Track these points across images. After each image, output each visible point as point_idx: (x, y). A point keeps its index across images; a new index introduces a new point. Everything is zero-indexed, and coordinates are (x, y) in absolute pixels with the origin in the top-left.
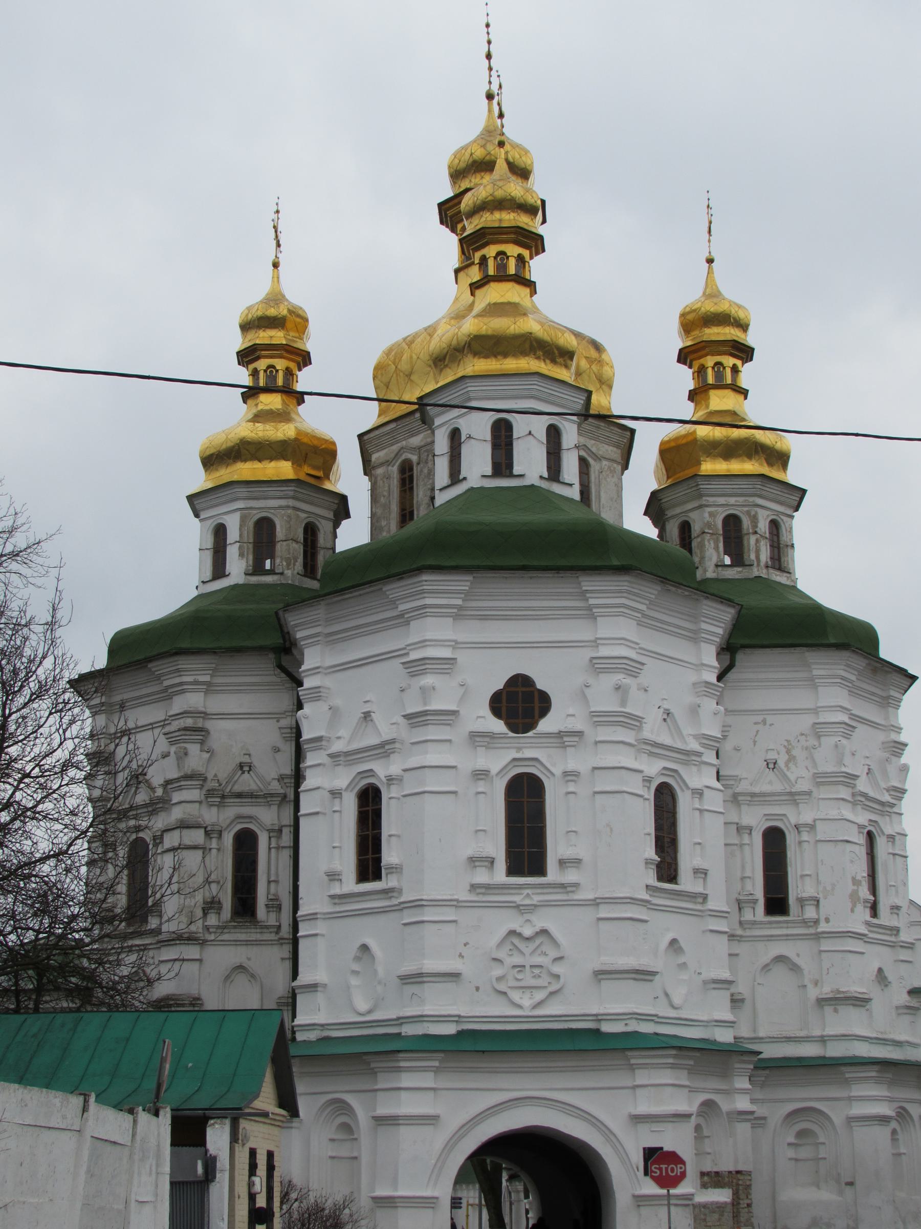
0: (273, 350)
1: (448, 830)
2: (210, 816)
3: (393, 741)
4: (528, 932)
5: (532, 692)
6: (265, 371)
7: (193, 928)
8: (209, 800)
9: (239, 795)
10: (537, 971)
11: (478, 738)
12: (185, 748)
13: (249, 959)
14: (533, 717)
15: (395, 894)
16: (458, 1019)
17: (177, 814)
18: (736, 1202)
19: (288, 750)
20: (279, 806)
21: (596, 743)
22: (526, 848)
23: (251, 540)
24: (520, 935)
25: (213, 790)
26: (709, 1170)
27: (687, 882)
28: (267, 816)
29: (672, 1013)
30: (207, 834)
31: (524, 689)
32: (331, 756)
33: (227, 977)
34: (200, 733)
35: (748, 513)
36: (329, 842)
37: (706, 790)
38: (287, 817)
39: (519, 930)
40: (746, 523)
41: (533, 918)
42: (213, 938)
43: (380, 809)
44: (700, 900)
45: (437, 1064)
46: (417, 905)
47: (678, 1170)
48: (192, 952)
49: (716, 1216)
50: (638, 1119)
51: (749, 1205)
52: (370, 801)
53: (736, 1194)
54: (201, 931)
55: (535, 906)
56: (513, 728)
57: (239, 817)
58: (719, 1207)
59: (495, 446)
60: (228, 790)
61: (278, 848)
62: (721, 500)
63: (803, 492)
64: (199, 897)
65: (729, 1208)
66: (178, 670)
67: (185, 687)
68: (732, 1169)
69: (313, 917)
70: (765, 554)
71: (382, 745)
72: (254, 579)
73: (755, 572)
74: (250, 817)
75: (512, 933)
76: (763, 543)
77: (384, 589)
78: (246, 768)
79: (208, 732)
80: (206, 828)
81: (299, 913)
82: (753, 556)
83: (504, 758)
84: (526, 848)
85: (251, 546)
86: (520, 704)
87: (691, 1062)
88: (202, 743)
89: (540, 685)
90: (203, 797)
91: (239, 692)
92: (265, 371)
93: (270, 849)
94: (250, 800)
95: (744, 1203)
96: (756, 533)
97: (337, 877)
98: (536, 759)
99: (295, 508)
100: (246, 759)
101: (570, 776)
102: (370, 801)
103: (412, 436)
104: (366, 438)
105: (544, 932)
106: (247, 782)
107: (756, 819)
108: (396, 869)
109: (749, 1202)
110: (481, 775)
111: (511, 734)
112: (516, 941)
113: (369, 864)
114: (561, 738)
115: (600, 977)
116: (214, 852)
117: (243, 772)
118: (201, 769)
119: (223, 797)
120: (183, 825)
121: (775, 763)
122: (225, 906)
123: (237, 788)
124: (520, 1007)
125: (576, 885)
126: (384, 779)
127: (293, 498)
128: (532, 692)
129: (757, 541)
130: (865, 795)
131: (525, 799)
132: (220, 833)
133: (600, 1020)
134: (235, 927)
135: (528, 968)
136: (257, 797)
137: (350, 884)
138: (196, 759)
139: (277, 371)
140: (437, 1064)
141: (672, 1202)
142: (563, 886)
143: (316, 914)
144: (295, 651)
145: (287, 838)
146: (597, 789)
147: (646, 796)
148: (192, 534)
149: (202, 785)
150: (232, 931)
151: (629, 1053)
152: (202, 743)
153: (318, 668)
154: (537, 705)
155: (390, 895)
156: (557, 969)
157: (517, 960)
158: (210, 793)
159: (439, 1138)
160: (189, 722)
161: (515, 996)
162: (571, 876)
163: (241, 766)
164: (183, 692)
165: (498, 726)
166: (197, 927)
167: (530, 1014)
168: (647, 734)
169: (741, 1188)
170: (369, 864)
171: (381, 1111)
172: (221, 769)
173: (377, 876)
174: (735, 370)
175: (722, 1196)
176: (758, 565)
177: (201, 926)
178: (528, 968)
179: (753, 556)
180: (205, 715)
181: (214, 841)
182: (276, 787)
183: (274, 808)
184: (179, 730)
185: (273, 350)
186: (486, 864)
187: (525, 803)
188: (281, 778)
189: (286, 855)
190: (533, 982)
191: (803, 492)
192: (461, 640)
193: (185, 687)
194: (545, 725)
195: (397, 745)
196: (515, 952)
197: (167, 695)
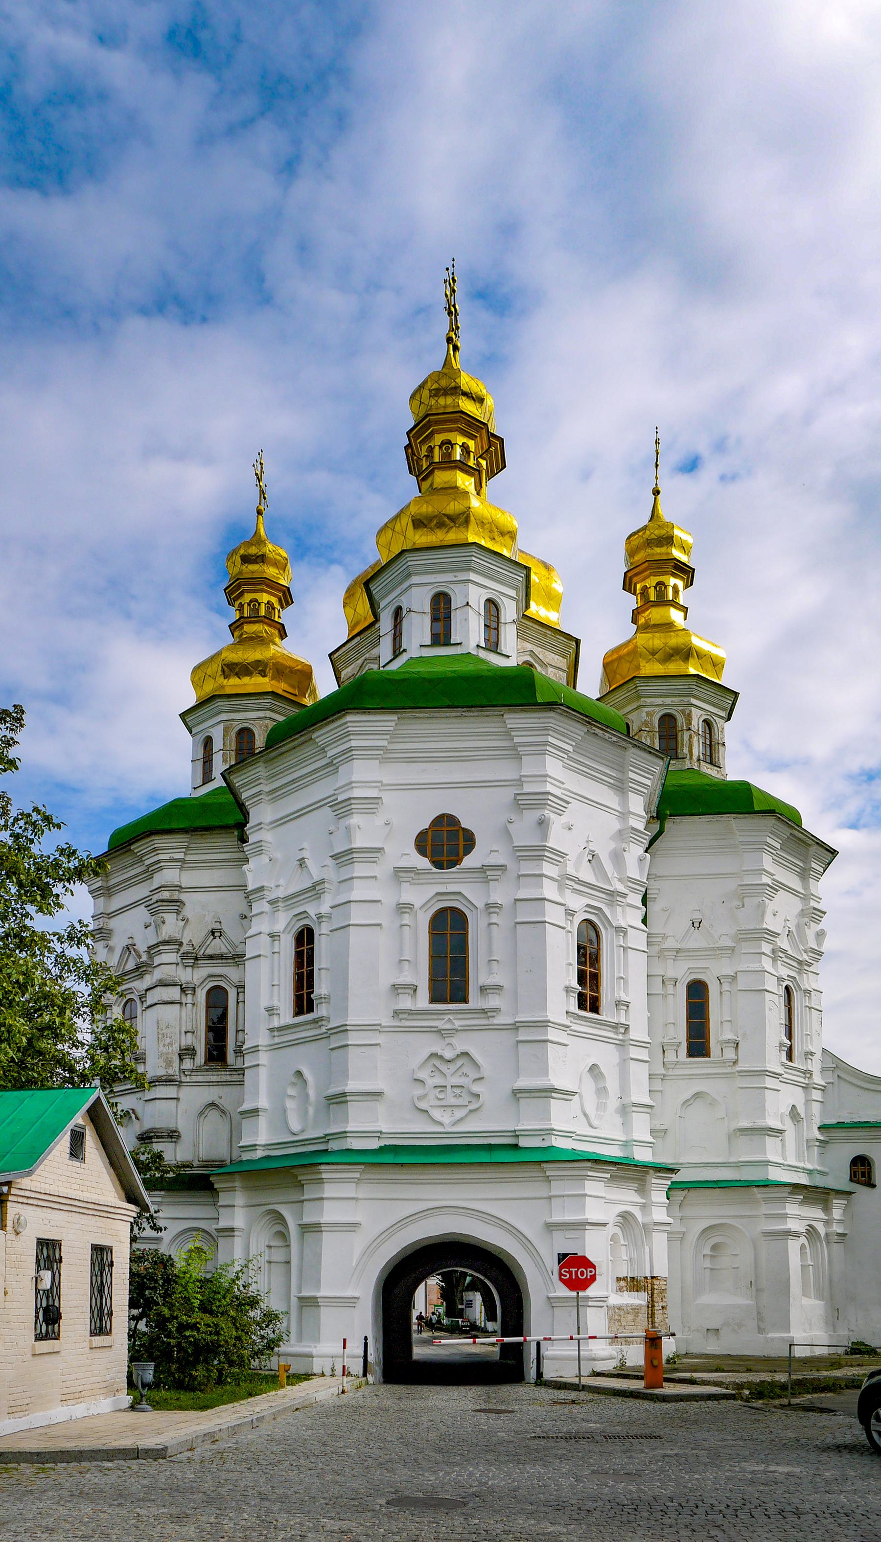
2: (185, 975)
3: (322, 882)
4: (448, 1054)
9: (211, 957)
10: (458, 1091)
11: (400, 874)
14: (458, 855)
15: (324, 1023)
16: (379, 1135)
18: (651, 1305)
21: (519, 876)
22: (450, 976)
25: (187, 953)
27: (607, 1013)
30: (183, 990)
32: (271, 902)
35: (683, 712)
37: (629, 929)
39: (440, 1053)
40: (681, 720)
41: (454, 1041)
44: (622, 1030)
45: (357, 1175)
46: (342, 1030)
47: (588, 1273)
49: (630, 1317)
50: (551, 1227)
55: (457, 1030)
56: (438, 865)
58: (636, 1310)
60: (201, 953)
62: (659, 701)
64: (176, 1048)
65: (644, 1310)
69: (255, 1049)
70: (698, 749)
71: (313, 887)
73: (687, 764)
75: (434, 1055)
76: (695, 739)
79: (182, 902)
80: (181, 985)
82: (686, 751)
83: (426, 893)
84: (450, 976)
87: (608, 1176)
88: (178, 912)
90: (179, 959)
91: (211, 868)
95: (658, 1306)
96: (690, 729)
97: (275, 1012)
98: (460, 893)
100: (217, 926)
101: (490, 907)
105: (466, 1054)
107: (683, 972)
108: (327, 998)
109: (664, 1304)
110: (403, 908)
111: (435, 870)
112: (437, 1063)
114: (484, 872)
115: (518, 1095)
118: (177, 936)
120: (163, 984)
123: (209, 952)
124: (441, 1124)
125: (497, 1010)
126: (315, 918)
129: (690, 736)
130: (784, 951)
133: (517, 1136)
135: (449, 1087)
137: (286, 1016)
138: (171, 926)
140: (357, 1175)
142: (484, 1011)
143: (258, 1046)
146: (518, 920)
147: (569, 928)
148: (184, 744)
151: (544, 1165)
152: (178, 912)
155: (320, 1023)
156: (476, 1088)
157: (438, 1081)
158: (185, 956)
159: (359, 1242)
161: (436, 1114)
162: (493, 1001)
165: (424, 863)
167: (450, 1130)
168: (571, 870)
169: (656, 1291)
171: (307, 1220)
172: (193, 935)
173: (311, 1009)
176: (691, 758)
178: (449, 1087)
179: (686, 751)
186: (409, 991)
187: (449, 934)
190: (453, 1101)
192: (390, 781)
194: (469, 861)
196: (437, 1074)
197: (149, 873)
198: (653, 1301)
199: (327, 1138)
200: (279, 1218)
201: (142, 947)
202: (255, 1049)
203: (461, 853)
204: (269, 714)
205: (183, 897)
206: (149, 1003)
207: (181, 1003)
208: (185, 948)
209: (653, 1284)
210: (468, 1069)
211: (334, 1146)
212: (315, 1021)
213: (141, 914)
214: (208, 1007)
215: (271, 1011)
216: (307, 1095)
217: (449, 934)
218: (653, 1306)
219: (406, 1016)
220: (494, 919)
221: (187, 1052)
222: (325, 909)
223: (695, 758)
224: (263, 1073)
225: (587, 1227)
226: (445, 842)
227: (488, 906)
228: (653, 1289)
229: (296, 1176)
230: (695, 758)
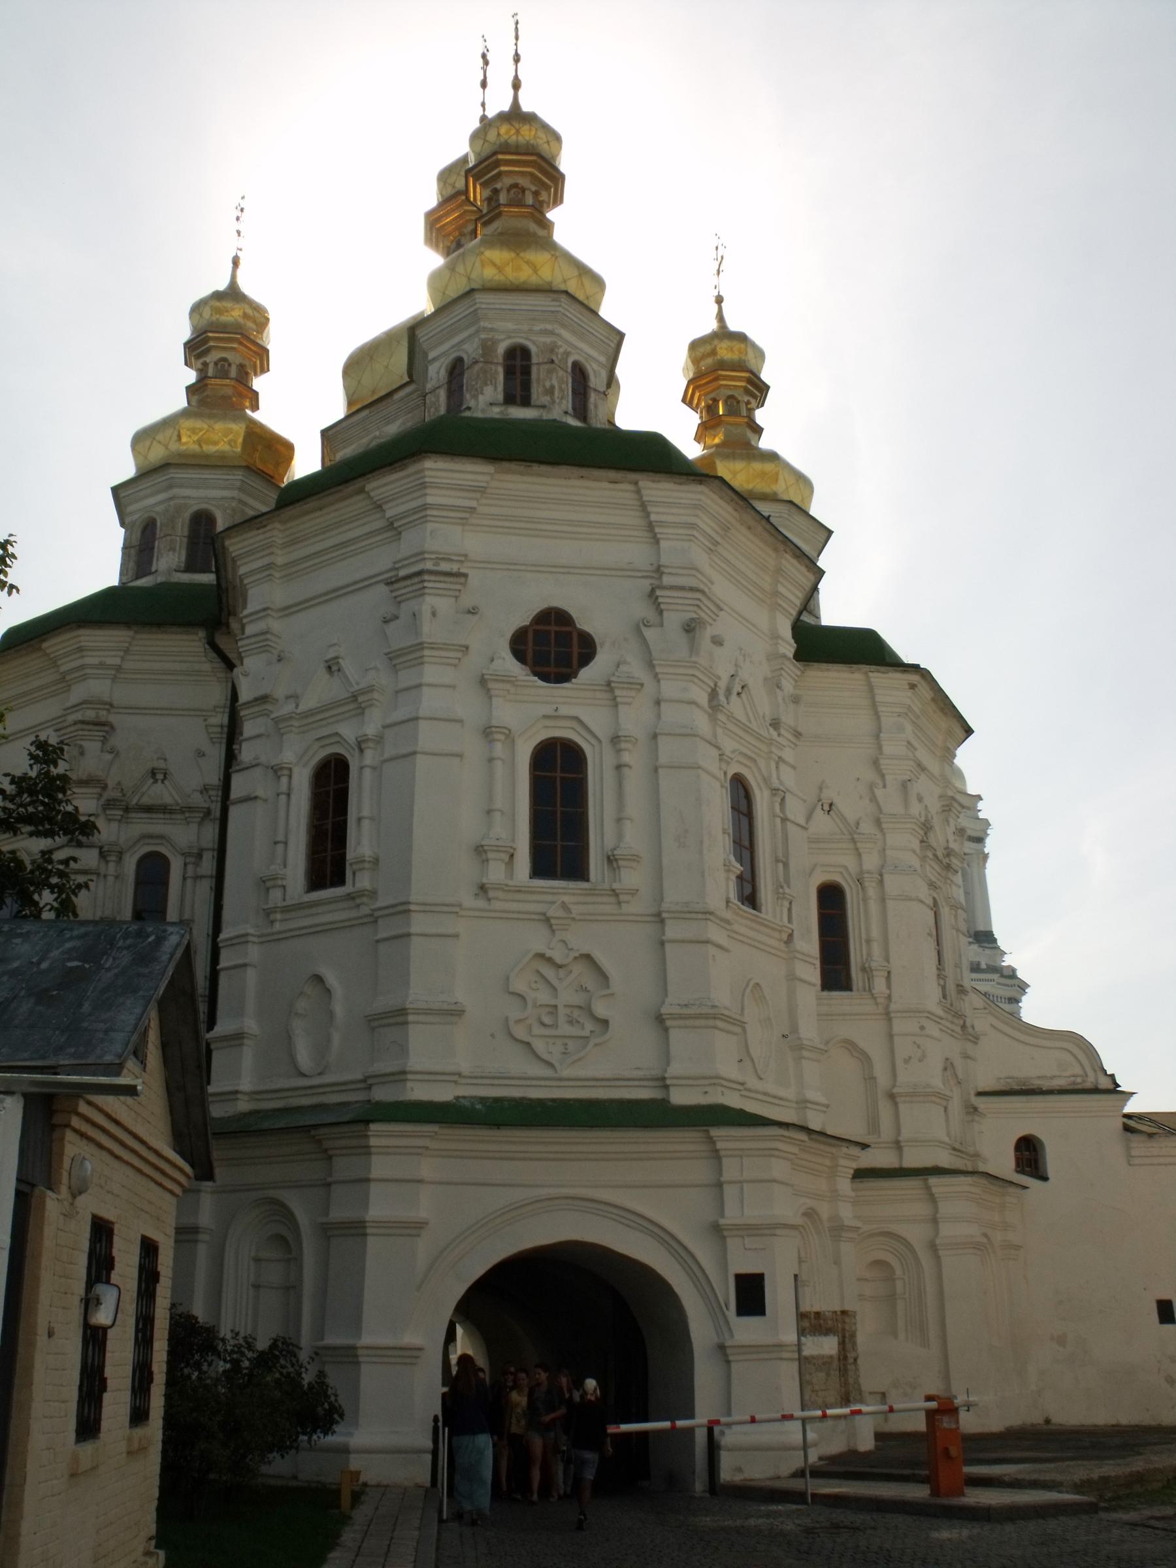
0: (226, 343)
1: (451, 801)
4: (558, 955)
5: (570, 633)
6: (216, 364)
8: (108, 812)
9: (148, 809)
12: (81, 746)
15: (365, 899)
19: (216, 754)
20: (200, 824)
23: (186, 534)
24: (550, 960)
25: (114, 800)
26: (808, 1309)
28: (183, 835)
29: (759, 1086)
30: (103, 855)
31: (557, 629)
36: (272, 831)
38: (210, 833)
43: (347, 788)
49: (822, 1375)
51: (855, 1360)
52: (332, 779)
53: (842, 1344)
55: (573, 919)
59: (509, 372)
60: (134, 802)
61: (197, 878)
63: (830, 532)
65: (835, 1364)
67: (88, 671)
68: (838, 1309)
69: (241, 940)
72: (186, 578)
74: (161, 837)
75: (541, 956)
77: (368, 487)
78: (160, 776)
79: (112, 727)
80: (101, 848)
81: (222, 936)
85: (185, 540)
86: (553, 646)
88: (104, 740)
89: (583, 624)
92: (216, 364)
93: (185, 879)
94: (161, 816)
97: (280, 882)
99: (240, 501)
100: (161, 764)
102: (332, 781)
103: (388, 423)
104: (330, 433)
106: (160, 793)
113: (328, 862)
116: (111, 879)
117: (156, 781)
119: (127, 810)
121: (831, 805)
123: (146, 800)
124: (550, 1064)
127: (240, 489)
128: (570, 633)
132: (120, 854)
136: (171, 812)
139: (230, 365)
144: (234, 625)
145: (208, 865)
149: (101, 795)
152: (104, 740)
153: (265, 609)
154: (576, 650)
155: (358, 901)
157: (543, 997)
160: (90, 714)
161: (539, 1046)
163: (153, 773)
164: (84, 678)
167: (565, 1073)
170: (328, 862)
171: (338, 1214)
174: (751, 411)
175: (828, 1346)
181: (112, 866)
182: (198, 800)
183: (194, 827)
184: (75, 723)
185: (226, 343)
187: (559, 776)
188: (205, 789)
189: (205, 889)
191: (830, 532)
193: (88, 671)
195: (375, 695)
198: (844, 1349)
199: (367, 1083)
200: (287, 1215)
202: (241, 940)
204: (235, 493)
205: (112, 718)
207: (98, 874)
208: (110, 794)
210: (590, 981)
211: (382, 1094)
212: (350, 897)
214: (138, 883)
215: (265, 884)
216: (331, 1014)
217: (559, 776)
218: (846, 1358)
219: (500, 894)
220: (626, 758)
222: (371, 730)
224: (251, 975)
225: (778, 1232)
227: (615, 740)
229: (319, 1141)
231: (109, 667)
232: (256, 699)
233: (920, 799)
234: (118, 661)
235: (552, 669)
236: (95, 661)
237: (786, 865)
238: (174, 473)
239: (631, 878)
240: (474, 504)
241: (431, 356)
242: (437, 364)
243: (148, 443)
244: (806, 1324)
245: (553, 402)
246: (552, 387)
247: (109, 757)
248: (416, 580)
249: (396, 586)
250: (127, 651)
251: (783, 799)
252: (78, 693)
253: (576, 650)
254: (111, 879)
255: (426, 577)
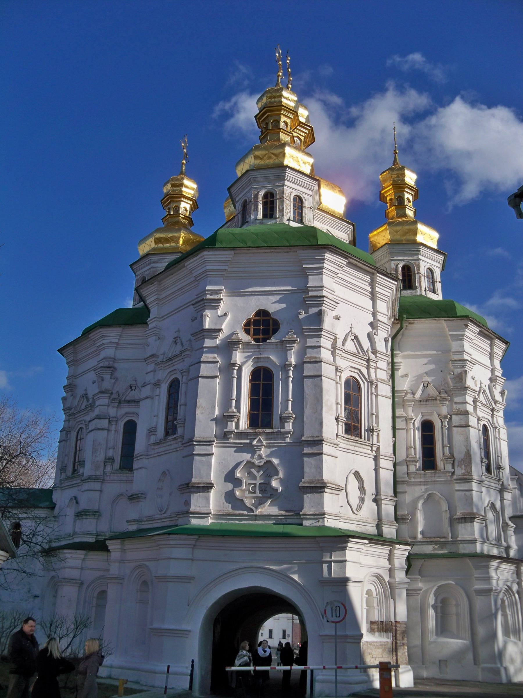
2: (112, 411)
7: (98, 473)
9: (129, 402)
12: (102, 377)
13: (127, 491)
17: (97, 412)
33: (114, 502)
34: (112, 369)
42: (108, 479)
48: (96, 485)
54: (102, 474)
56: (256, 340)
57: (127, 413)
60: (123, 399)
66: (102, 337)
73: (418, 293)
74: (133, 413)
78: (133, 388)
82: (417, 284)
88: (112, 374)
94: (134, 404)
97: (155, 433)
100: (134, 383)
111: (253, 342)
116: (113, 432)
117: (132, 390)
122: (116, 461)
123: (128, 398)
131: (261, 382)
134: (120, 473)
138: (107, 384)
141: (338, 640)
150: (119, 475)
154: (271, 327)
158: (113, 401)
160: (106, 364)
164: (104, 349)
166: (99, 473)
176: (421, 289)
177: (102, 472)
180: (114, 360)
181: (114, 426)
201: (90, 396)
203: (271, 332)
205: (116, 365)
206: (90, 429)
208: (114, 396)
209: (395, 626)
213: (92, 376)
217: (263, 383)
221: (110, 460)
223: (423, 289)
226: (263, 326)
228: (396, 630)
230: (423, 289)
231: (113, 343)
232: (150, 356)
233: (473, 378)
234: (116, 341)
235: (261, 336)
236: (108, 341)
237: (377, 417)
238: (151, 258)
239: (289, 426)
240: (223, 268)
241: (237, 199)
242: (239, 203)
243: (143, 245)
244: (375, 627)
245: (283, 215)
246: (283, 209)
247: (113, 381)
248: (202, 303)
249: (195, 306)
250: (120, 336)
251: (376, 386)
252: (102, 355)
253: (271, 327)
254: (113, 432)
255: (205, 301)
